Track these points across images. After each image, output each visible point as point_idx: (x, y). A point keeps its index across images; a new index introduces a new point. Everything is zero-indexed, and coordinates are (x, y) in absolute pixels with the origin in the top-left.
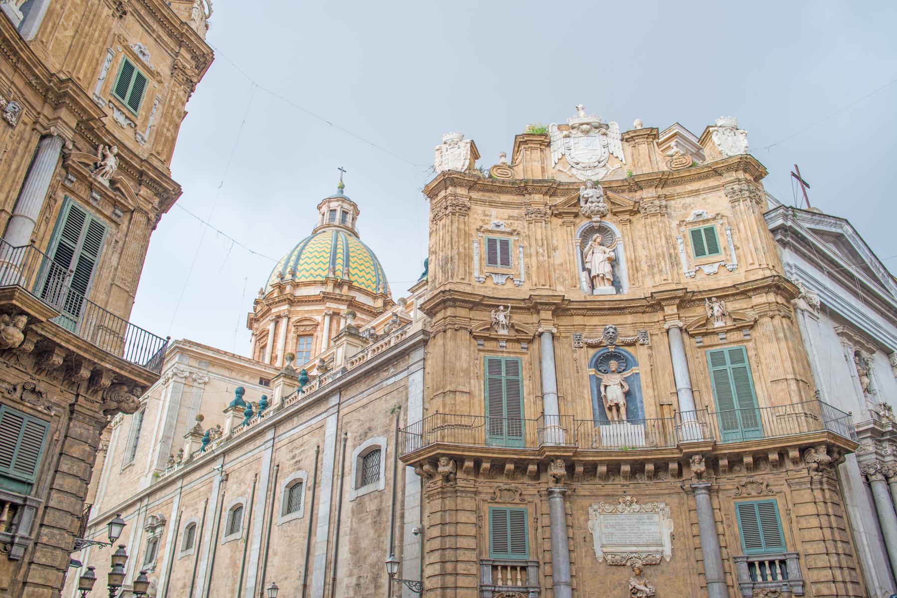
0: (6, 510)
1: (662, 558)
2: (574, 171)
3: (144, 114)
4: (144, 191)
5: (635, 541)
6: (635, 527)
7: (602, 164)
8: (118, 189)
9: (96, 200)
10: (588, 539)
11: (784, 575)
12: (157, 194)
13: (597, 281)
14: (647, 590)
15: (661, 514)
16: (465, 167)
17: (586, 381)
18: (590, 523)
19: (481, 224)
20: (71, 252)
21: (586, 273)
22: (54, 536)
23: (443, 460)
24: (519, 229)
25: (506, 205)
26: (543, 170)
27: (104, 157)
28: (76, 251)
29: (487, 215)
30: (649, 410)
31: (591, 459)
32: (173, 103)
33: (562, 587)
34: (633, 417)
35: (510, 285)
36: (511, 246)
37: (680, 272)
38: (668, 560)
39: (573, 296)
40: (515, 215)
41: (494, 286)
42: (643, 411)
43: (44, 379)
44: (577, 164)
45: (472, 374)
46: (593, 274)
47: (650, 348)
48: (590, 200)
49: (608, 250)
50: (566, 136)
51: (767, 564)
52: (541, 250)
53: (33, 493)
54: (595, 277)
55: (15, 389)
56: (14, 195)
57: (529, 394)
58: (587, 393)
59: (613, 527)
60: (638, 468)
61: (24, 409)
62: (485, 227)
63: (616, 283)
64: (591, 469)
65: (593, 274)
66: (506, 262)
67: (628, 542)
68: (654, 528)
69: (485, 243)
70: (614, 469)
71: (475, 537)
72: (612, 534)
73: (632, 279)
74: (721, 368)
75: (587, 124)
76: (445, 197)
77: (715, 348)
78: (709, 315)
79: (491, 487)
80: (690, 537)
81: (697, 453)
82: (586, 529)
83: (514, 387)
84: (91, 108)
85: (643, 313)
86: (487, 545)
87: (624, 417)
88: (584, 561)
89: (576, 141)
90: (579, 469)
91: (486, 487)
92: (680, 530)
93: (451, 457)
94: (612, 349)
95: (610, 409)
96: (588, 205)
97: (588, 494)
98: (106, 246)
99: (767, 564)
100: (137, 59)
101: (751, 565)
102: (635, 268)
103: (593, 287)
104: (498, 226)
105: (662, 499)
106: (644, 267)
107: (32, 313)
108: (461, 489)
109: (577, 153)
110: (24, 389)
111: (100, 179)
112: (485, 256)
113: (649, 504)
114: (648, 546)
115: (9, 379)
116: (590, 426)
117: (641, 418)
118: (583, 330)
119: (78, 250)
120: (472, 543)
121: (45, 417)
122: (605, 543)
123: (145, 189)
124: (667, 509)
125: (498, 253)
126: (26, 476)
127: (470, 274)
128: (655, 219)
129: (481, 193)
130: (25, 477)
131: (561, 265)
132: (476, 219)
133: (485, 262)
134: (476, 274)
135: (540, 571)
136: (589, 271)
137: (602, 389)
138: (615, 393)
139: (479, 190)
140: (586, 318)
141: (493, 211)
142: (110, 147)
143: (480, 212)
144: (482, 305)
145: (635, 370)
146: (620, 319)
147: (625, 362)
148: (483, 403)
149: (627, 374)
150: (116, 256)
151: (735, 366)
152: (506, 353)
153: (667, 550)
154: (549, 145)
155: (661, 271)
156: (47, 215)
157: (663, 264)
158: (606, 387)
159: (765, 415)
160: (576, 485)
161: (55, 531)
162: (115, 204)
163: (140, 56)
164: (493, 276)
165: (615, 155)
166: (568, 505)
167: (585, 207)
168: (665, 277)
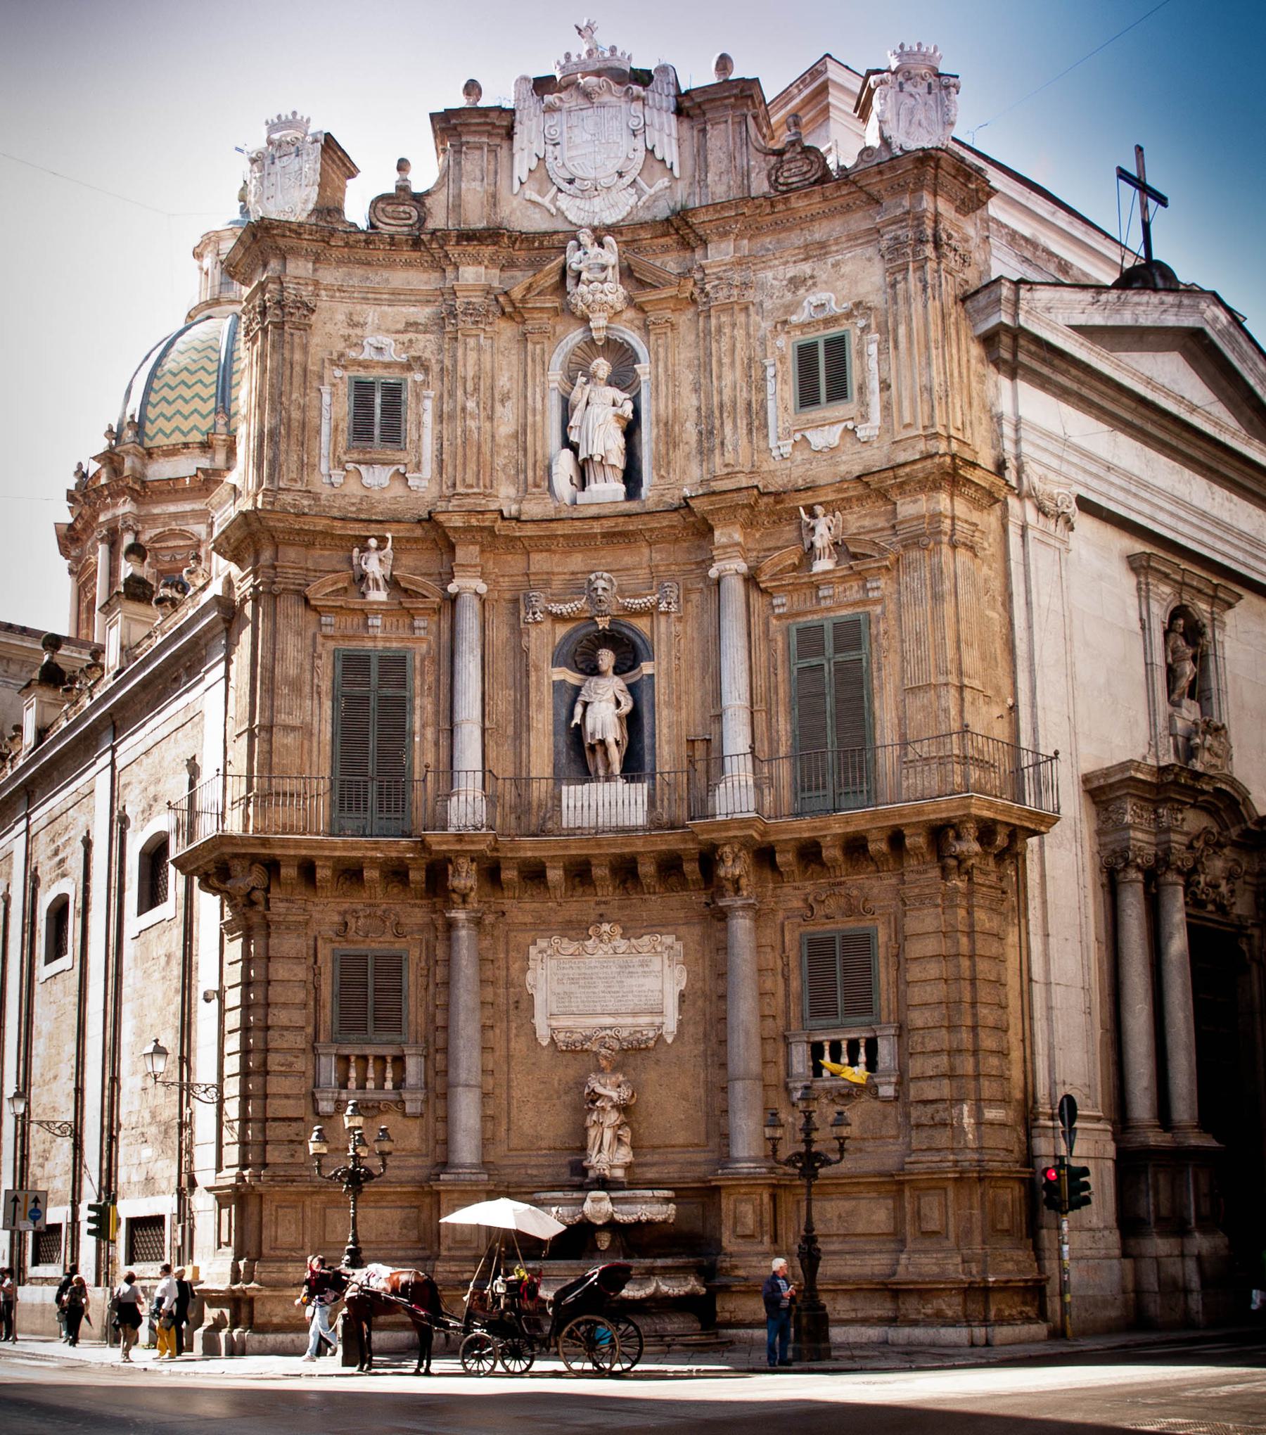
1: (660, 1038)
2: (564, 202)
5: (611, 1006)
6: (611, 986)
7: (627, 180)
10: (523, 1006)
11: (871, 1065)
13: (591, 472)
14: (614, 1095)
15: (665, 956)
16: (311, 206)
17: (547, 697)
18: (529, 975)
19: (340, 346)
21: (567, 454)
23: (237, 867)
24: (427, 355)
25: (397, 297)
26: (494, 200)
29: (356, 325)
30: (666, 751)
31: (529, 854)
33: (460, 1089)
34: (634, 765)
35: (398, 489)
36: (408, 395)
37: (762, 444)
38: (669, 1040)
39: (533, 509)
40: (422, 320)
41: (364, 493)
42: (654, 755)
44: (571, 182)
45: (307, 689)
46: (583, 455)
47: (680, 619)
48: (584, 276)
49: (620, 396)
50: (551, 109)
51: (844, 1045)
52: (471, 405)
54: (585, 460)
57: (423, 726)
58: (543, 722)
59: (573, 981)
60: (626, 871)
62: (352, 354)
63: (631, 476)
64: (534, 874)
65: (583, 455)
66: (394, 433)
67: (599, 1010)
68: (651, 984)
69: (344, 389)
70: (580, 872)
71: (305, 1005)
72: (569, 995)
73: (663, 463)
74: (815, 661)
75: (598, 73)
76: (262, 287)
77: (810, 618)
78: (807, 544)
79: (339, 913)
80: (714, 998)
81: (729, 841)
82: (523, 986)
83: (395, 712)
85: (677, 540)
86: (328, 1020)
87: (617, 768)
88: (513, 1044)
89: (574, 120)
90: (509, 874)
91: (327, 910)
92: (699, 985)
93: (254, 859)
94: (603, 623)
95: (592, 748)
96: (583, 288)
97: (529, 919)
99: (844, 1045)
101: (817, 1050)
102: (669, 437)
103: (583, 485)
104: (379, 349)
105: (670, 929)
106: (690, 432)
108: (276, 918)
109: (573, 153)
112: (345, 425)
113: (646, 938)
114: (635, 1014)
116: (543, 789)
117: (648, 770)
118: (548, 583)
120: (298, 1017)
122: (555, 1011)
124: (678, 946)
125: (378, 415)
127: (314, 467)
128: (723, 319)
129: (343, 270)
131: (515, 436)
132: (330, 335)
133: (343, 440)
134: (324, 468)
135: (430, 1064)
136: (574, 448)
137: (579, 710)
138: (604, 714)
139: (340, 262)
140: (556, 558)
141: (371, 314)
143: (340, 317)
144: (333, 536)
145: (647, 668)
146: (628, 560)
147: (629, 653)
148: (328, 748)
149: (633, 676)
151: (840, 657)
152: (381, 636)
153: (670, 1024)
154: (510, 134)
155: (722, 443)
157: (728, 429)
158: (586, 705)
159: (887, 759)
160: (508, 904)
164: (362, 468)
165: (659, 155)
166: (486, 943)
167: (580, 294)
168: (729, 457)
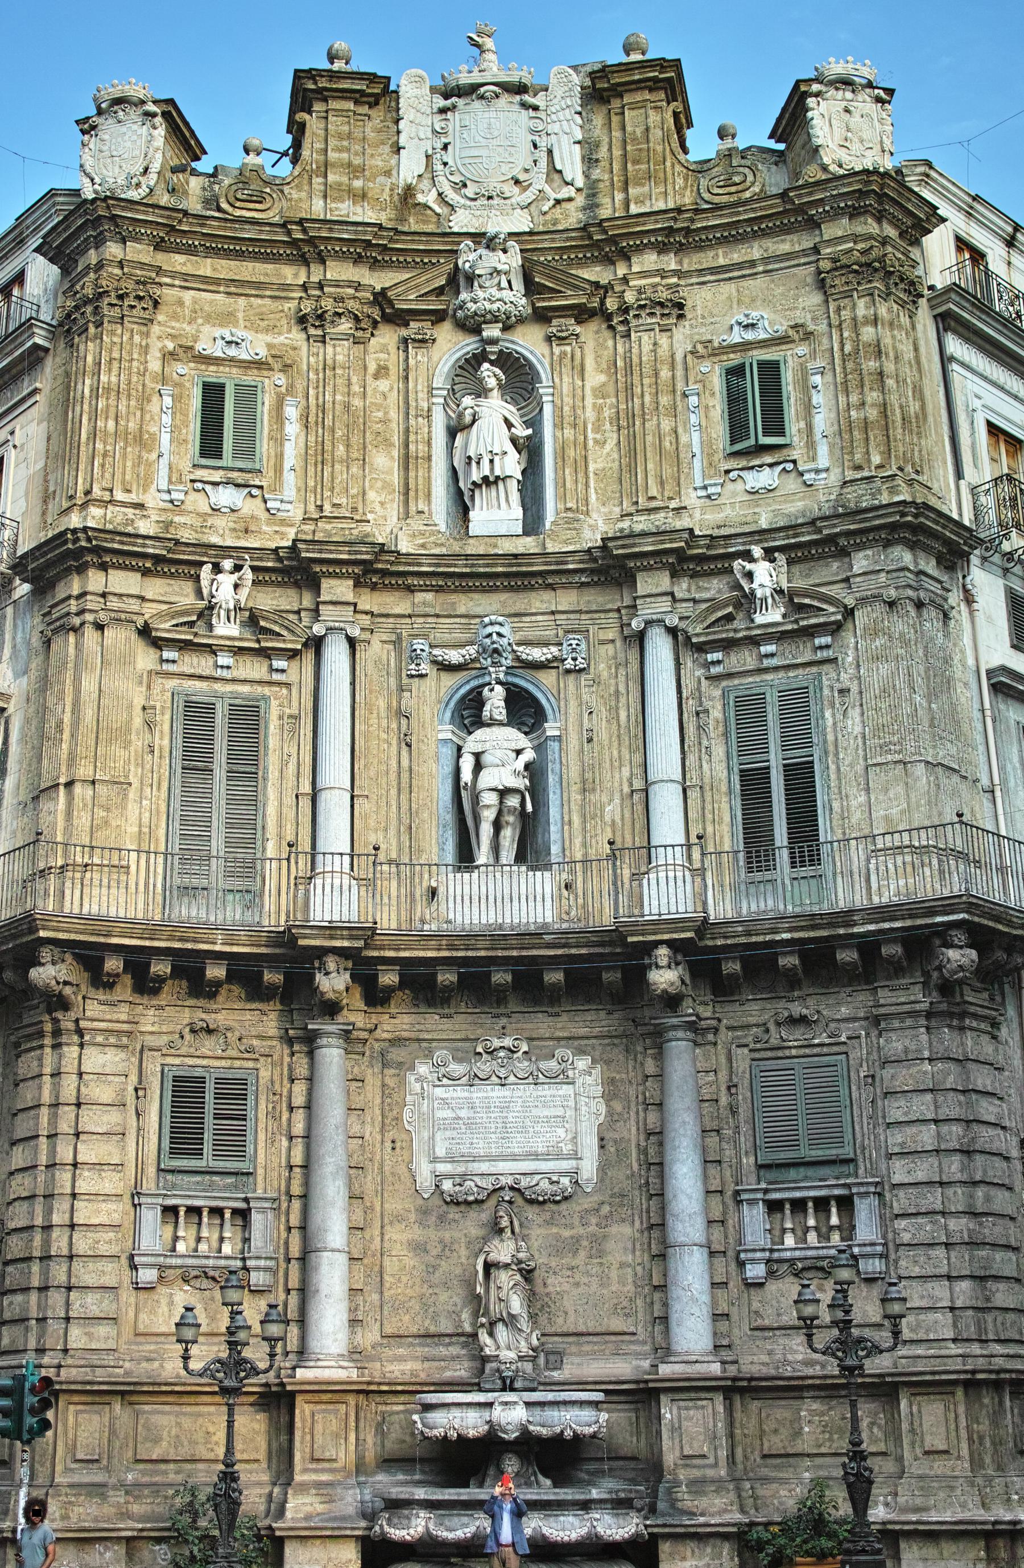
0: (834, 1210)
3: (802, 425)
4: (861, 561)
8: (801, 608)
9: (772, 655)
12: (887, 544)
20: (765, 773)
22: (921, 1227)
27: (750, 575)
28: (773, 763)
32: (848, 348)
43: (811, 991)
53: (861, 1171)
55: (767, 1031)
56: (638, 758)
61: (794, 1052)
84: (662, 542)
98: (828, 714)
100: (745, 346)
107: (666, 937)
110: (778, 1024)
111: (759, 619)
115: (752, 1020)
119: (775, 761)
121: (835, 1049)
123: (861, 554)
126: (834, 1152)
130: (832, 1153)
142: (747, 556)
150: (855, 713)
156: (705, 743)
161: (920, 1220)
162: (809, 632)
163: (750, 336)
